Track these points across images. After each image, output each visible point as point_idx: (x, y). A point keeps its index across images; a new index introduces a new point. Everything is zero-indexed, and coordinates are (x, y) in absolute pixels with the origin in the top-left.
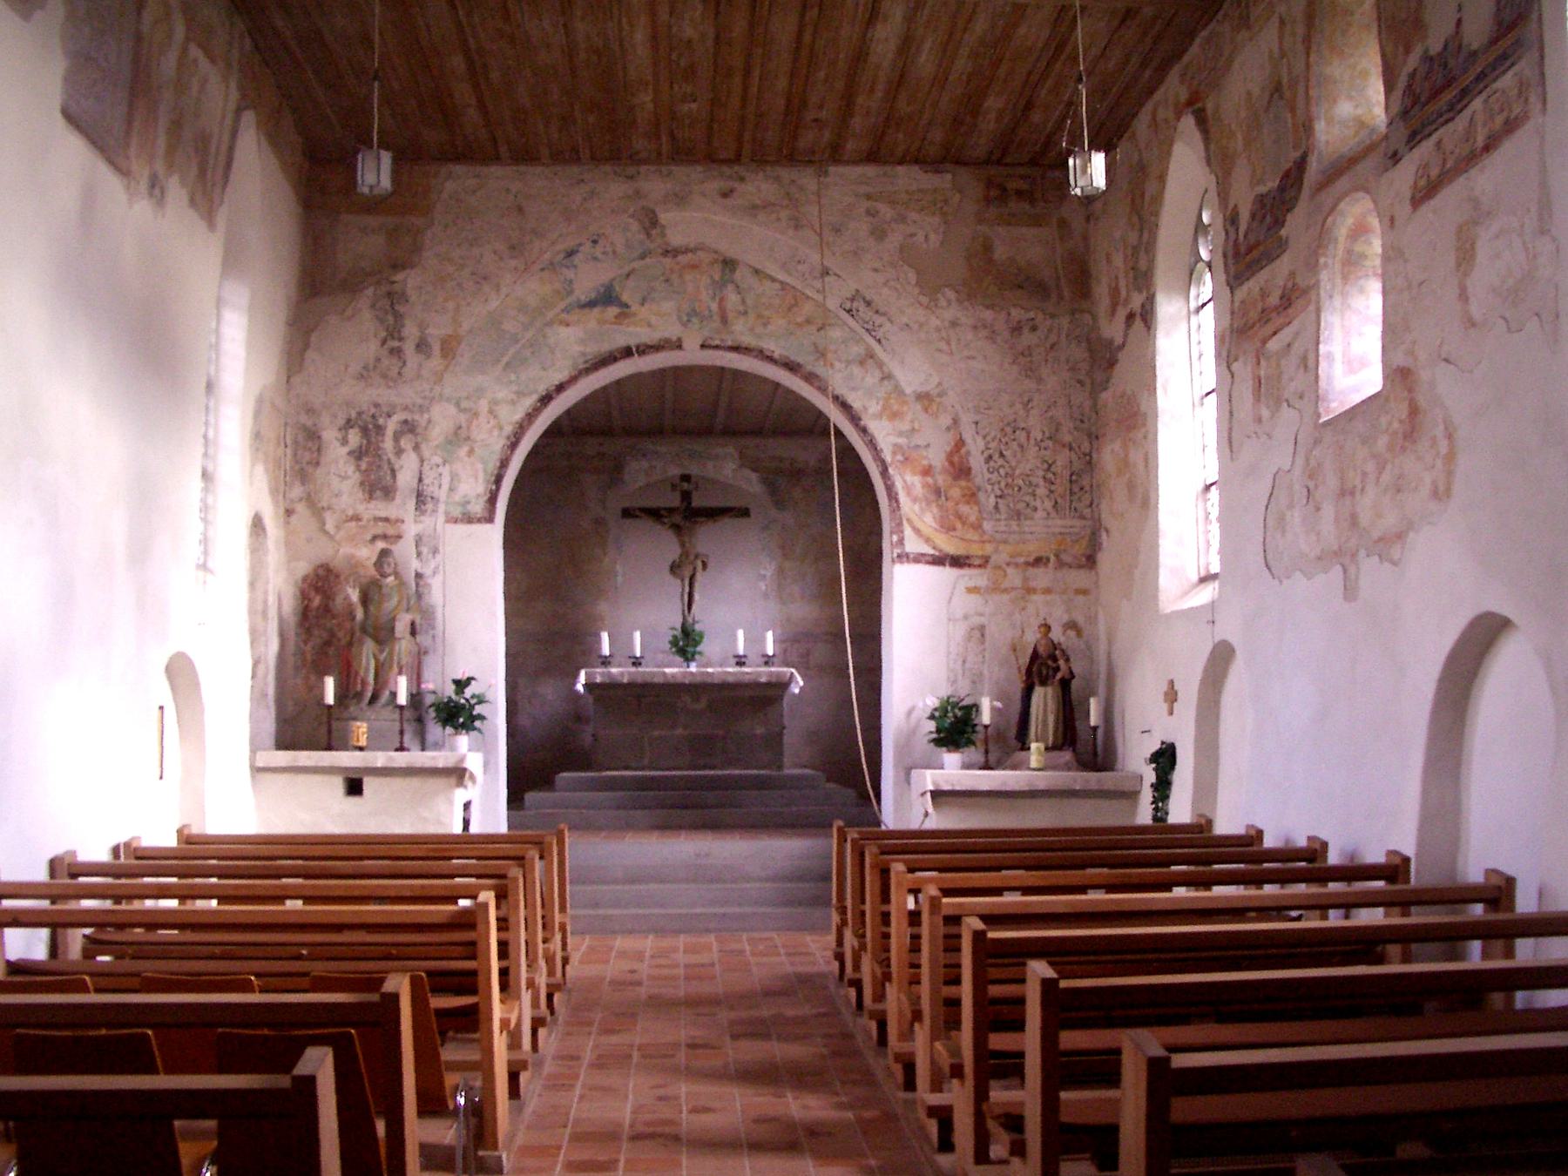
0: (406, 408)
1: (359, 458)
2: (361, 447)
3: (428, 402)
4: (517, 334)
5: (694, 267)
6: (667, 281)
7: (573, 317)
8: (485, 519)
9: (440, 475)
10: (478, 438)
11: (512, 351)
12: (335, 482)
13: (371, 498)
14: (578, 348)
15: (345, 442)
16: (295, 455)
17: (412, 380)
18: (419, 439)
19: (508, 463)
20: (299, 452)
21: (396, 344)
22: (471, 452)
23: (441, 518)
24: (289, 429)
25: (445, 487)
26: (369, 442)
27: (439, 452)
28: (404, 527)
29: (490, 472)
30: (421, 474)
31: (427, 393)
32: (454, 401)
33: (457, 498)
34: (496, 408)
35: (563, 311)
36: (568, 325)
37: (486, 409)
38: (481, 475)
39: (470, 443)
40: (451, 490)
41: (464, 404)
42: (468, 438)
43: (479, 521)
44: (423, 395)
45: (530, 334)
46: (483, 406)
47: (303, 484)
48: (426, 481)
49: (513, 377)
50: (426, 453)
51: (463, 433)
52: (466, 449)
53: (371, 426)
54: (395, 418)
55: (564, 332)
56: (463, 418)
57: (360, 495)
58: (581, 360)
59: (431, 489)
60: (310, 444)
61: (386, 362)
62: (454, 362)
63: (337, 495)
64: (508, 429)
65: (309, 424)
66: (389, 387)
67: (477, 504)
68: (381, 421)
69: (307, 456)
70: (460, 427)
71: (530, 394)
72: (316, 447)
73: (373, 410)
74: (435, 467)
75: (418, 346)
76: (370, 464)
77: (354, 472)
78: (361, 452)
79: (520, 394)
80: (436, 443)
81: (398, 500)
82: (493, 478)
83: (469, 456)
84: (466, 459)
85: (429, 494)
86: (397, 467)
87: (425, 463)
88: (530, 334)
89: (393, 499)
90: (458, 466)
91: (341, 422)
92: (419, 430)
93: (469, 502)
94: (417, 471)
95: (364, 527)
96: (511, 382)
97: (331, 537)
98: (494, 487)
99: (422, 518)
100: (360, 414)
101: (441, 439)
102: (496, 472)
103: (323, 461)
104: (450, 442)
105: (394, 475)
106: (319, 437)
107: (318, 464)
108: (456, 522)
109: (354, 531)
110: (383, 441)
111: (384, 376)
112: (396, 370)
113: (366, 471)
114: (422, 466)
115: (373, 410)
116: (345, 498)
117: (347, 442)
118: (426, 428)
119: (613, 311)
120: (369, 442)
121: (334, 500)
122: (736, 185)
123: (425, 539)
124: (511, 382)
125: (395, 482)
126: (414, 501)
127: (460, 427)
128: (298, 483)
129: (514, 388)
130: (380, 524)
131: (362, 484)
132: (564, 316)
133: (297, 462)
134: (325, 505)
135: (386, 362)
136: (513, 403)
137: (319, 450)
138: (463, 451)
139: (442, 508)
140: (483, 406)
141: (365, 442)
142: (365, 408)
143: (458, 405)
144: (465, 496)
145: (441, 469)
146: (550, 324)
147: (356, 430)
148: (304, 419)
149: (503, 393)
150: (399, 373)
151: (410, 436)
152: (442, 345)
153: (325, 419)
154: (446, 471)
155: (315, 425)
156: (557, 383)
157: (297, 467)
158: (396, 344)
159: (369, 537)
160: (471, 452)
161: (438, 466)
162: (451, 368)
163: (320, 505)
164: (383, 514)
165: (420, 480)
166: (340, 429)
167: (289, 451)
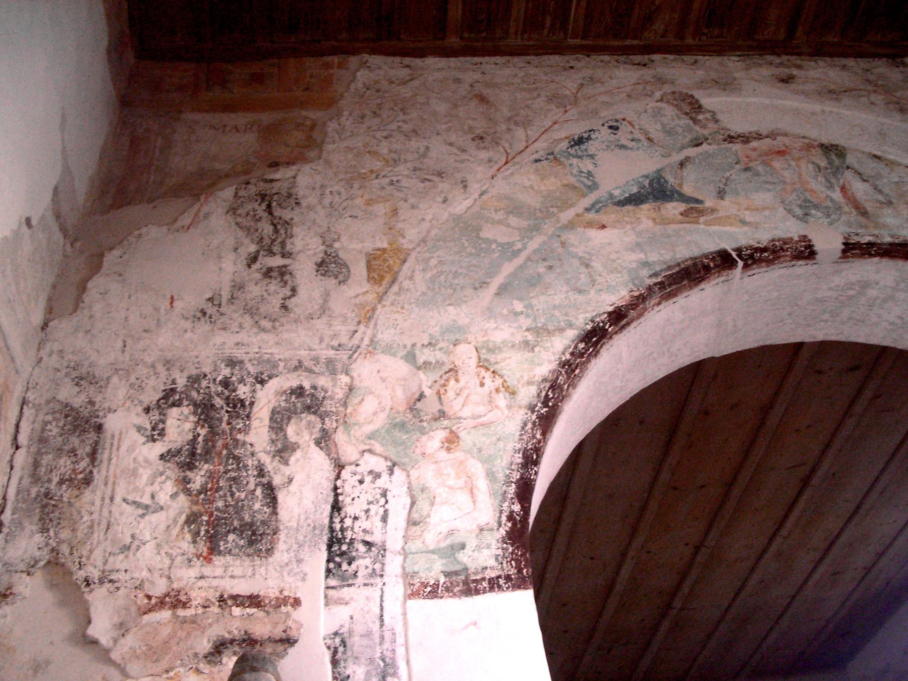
0: (299, 366)
1: (190, 466)
2: (193, 442)
3: (343, 356)
4: (510, 245)
5: (781, 153)
6: (747, 169)
7: (603, 218)
8: (508, 578)
9: (384, 494)
10: (467, 412)
11: (508, 268)
12: (125, 516)
13: (214, 550)
14: (633, 258)
15: (157, 433)
16: (36, 465)
17: (311, 317)
18: (329, 424)
19: (539, 456)
20: (46, 460)
21: (277, 261)
22: (452, 441)
23: (395, 589)
24: (28, 412)
25: (398, 518)
26: (213, 433)
27: (378, 448)
28: (298, 614)
29: (501, 476)
30: (337, 495)
31: (344, 339)
32: (403, 353)
33: (431, 537)
34: (492, 358)
35: (587, 210)
36: (603, 227)
37: (473, 362)
38: (482, 484)
39: (446, 423)
40: (412, 523)
41: (423, 356)
42: (442, 414)
43: (494, 585)
44: (335, 343)
45: (534, 244)
46: (465, 356)
47: (44, 530)
48: (350, 509)
49: (519, 306)
50: (348, 452)
51: (430, 406)
52: (440, 435)
53: (218, 402)
54: (273, 385)
55: (596, 236)
56: (425, 380)
57: (186, 545)
58: (645, 272)
59: (366, 525)
60: (75, 441)
61: (254, 291)
62: (395, 288)
63: (126, 548)
64: (528, 394)
65: (78, 401)
66: (264, 330)
67: (478, 548)
68: (243, 391)
69: (65, 464)
70: (421, 397)
71: (561, 330)
72: (88, 449)
73: (226, 372)
74: (368, 479)
75: (320, 265)
76: (211, 475)
77: (174, 496)
78: (193, 454)
79: (541, 331)
80: (368, 429)
81: (281, 554)
82: (513, 488)
83: (449, 450)
84: (443, 454)
85: (360, 536)
86: (277, 481)
87: (345, 474)
88: (534, 244)
89: (270, 551)
90: (425, 474)
91: (152, 396)
92: (328, 406)
93: (463, 547)
94: (328, 486)
95: (193, 620)
96: (516, 314)
97: (103, 655)
98: (517, 508)
99: (346, 592)
100: (194, 380)
101: (381, 420)
102: (516, 476)
103: (98, 477)
104: (402, 426)
105: (272, 500)
106: (99, 428)
107: (88, 481)
108: (434, 592)
109: (166, 632)
110: (246, 430)
111: (251, 311)
112: (276, 302)
113: (204, 490)
114: (338, 477)
115: (226, 372)
116: (148, 551)
117: (162, 433)
118: (345, 405)
119: (674, 209)
120: (213, 433)
121: (119, 562)
122: (795, 72)
123: (356, 642)
124: (516, 314)
125: (275, 513)
126: (324, 555)
127: (421, 397)
128: (31, 527)
129: (525, 322)
130: (237, 611)
131: (192, 519)
132: (591, 216)
133: (36, 478)
134: (95, 574)
135: (254, 291)
136: (527, 346)
137: (93, 455)
138: (434, 440)
139: (393, 565)
140: (465, 356)
141: (203, 432)
142: (207, 369)
143: (410, 357)
144: (451, 533)
145: (380, 483)
146: (570, 226)
147: (186, 410)
148: (67, 393)
149: (502, 333)
150: (284, 307)
151: (312, 418)
152: (368, 262)
153: (118, 391)
154: (397, 485)
155: (92, 403)
156: (611, 309)
157: (34, 491)
158: (277, 261)
159: (205, 645)
160: (452, 441)
161: (378, 476)
162: (391, 297)
163: (81, 574)
164: (243, 588)
165: (336, 507)
166: (147, 410)
167: (21, 457)
